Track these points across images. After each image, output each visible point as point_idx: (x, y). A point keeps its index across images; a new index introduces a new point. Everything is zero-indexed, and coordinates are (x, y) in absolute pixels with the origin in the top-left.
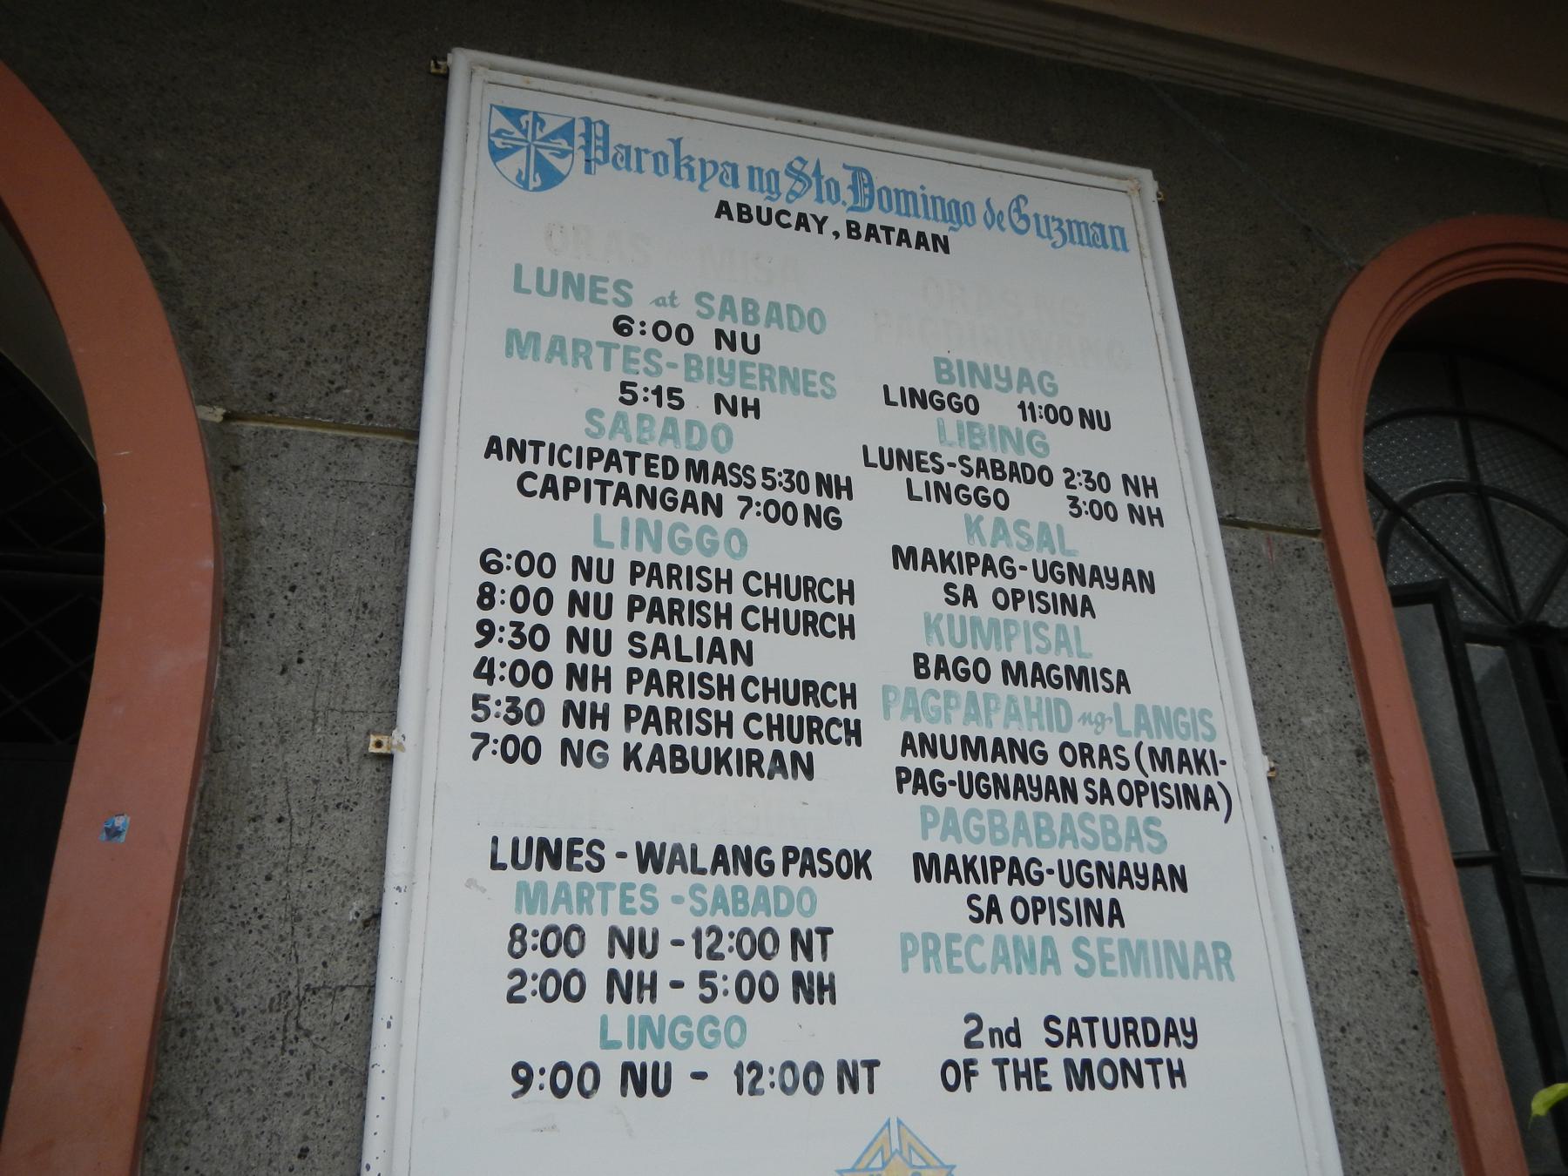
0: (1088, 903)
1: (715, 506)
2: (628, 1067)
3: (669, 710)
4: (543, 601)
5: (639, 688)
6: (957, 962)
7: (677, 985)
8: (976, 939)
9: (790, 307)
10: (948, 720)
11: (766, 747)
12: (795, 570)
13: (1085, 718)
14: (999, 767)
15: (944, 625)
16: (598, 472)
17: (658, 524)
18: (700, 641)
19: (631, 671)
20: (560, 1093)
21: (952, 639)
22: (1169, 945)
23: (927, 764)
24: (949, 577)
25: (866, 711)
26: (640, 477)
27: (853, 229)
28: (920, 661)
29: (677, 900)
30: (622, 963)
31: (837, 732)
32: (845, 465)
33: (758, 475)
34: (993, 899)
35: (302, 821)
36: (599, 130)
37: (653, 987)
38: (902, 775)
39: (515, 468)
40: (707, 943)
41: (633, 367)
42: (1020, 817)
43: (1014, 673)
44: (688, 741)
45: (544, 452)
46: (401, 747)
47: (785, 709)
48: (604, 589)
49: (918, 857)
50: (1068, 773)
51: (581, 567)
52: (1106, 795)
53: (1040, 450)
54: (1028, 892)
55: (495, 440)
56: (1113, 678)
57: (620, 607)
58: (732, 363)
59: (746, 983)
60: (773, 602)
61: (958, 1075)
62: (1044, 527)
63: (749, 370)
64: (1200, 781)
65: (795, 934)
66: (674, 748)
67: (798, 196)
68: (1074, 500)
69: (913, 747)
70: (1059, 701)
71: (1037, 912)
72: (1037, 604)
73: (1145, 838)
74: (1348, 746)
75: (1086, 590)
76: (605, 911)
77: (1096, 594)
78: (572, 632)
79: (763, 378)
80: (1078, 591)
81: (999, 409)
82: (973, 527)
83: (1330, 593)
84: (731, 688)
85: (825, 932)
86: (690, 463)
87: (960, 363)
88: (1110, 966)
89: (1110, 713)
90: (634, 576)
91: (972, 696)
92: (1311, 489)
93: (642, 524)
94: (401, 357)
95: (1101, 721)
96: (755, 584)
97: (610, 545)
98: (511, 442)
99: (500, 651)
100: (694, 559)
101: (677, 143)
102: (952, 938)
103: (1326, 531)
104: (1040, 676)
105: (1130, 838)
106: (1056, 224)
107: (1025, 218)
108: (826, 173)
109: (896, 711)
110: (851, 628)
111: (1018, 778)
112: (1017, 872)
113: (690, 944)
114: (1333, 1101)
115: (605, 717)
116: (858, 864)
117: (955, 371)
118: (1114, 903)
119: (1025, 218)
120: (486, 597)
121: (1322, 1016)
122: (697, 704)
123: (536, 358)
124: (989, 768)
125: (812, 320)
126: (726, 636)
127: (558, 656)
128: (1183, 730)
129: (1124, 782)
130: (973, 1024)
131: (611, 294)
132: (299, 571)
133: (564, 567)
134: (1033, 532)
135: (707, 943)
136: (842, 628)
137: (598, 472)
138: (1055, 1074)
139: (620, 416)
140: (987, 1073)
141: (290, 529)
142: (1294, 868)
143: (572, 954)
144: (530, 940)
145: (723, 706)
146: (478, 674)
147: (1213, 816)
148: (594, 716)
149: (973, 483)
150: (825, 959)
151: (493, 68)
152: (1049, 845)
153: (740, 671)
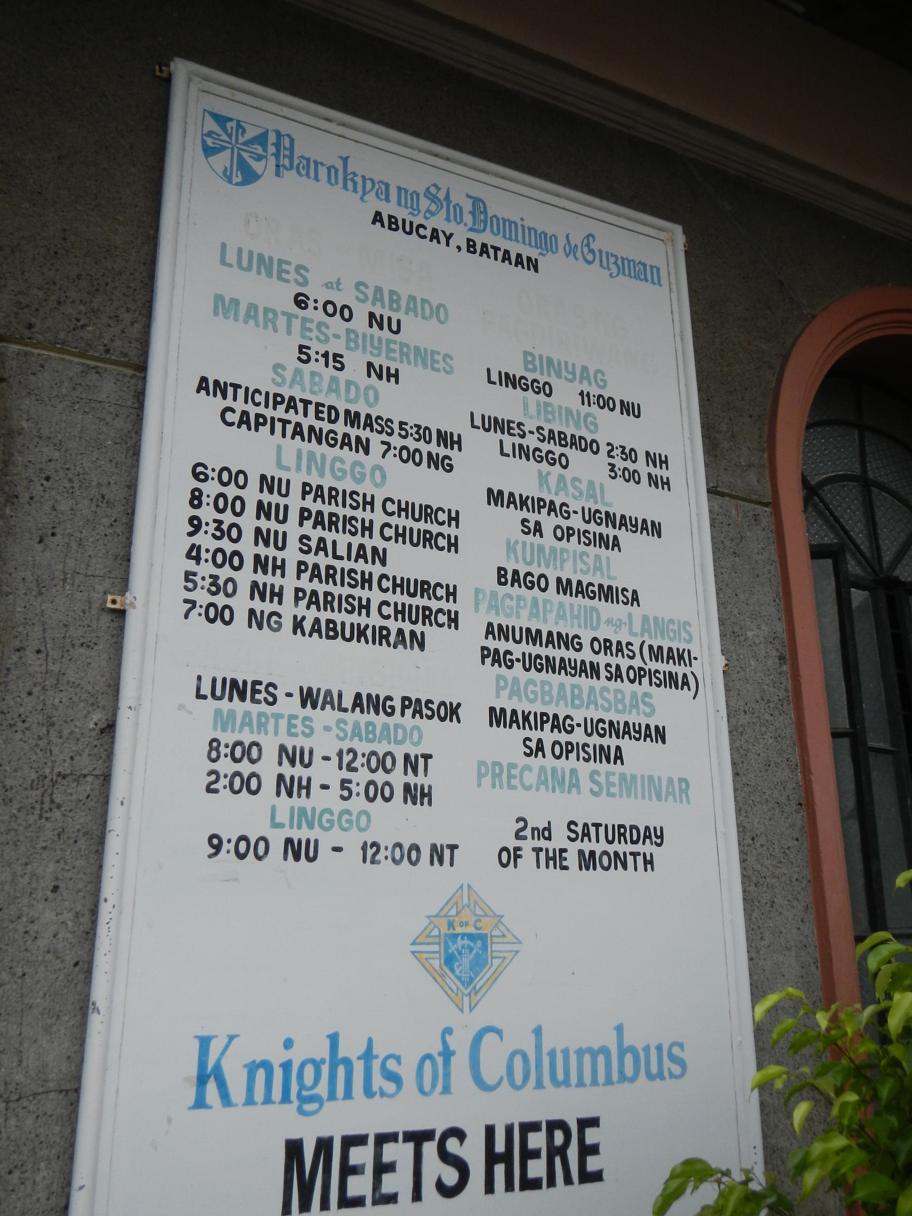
0: (601, 747)
1: (364, 446)
2: (289, 841)
3: (326, 594)
4: (237, 506)
5: (306, 576)
6: (514, 782)
7: (325, 787)
8: (528, 768)
9: (424, 301)
10: (518, 616)
11: (393, 625)
12: (419, 499)
13: (609, 622)
14: (550, 652)
15: (519, 548)
16: (280, 412)
17: (323, 456)
18: (350, 545)
19: (300, 563)
20: (241, 856)
21: (524, 559)
22: (651, 778)
23: (502, 646)
24: (524, 514)
25: (462, 606)
26: (311, 420)
27: (471, 246)
29: (327, 729)
30: (287, 770)
31: (442, 619)
32: (458, 425)
33: (396, 426)
34: (540, 741)
35: (54, 654)
36: (287, 142)
37: (308, 787)
38: (485, 653)
39: (219, 403)
41: (308, 334)
42: (562, 686)
43: (564, 586)
44: (338, 617)
45: (241, 393)
46: (132, 605)
47: (408, 600)
49: (492, 710)
50: (595, 659)
52: (619, 676)
53: (592, 428)
54: (563, 737)
55: (204, 380)
56: (629, 595)
57: (293, 515)
58: (380, 339)
59: (372, 789)
60: (403, 522)
62: (591, 484)
63: (392, 346)
64: (680, 670)
65: (407, 757)
66: (329, 621)
67: (433, 214)
68: (613, 466)
69: (493, 633)
70: (593, 609)
71: (568, 752)
72: (583, 539)
73: (641, 706)
75: (616, 532)
76: (276, 733)
77: (623, 535)
78: (258, 531)
80: (610, 532)
82: (543, 479)
83: (773, 547)
84: (370, 581)
85: (427, 757)
86: (347, 412)
87: (541, 357)
88: (612, 790)
89: (625, 619)
90: (304, 494)
91: (535, 599)
92: (767, 473)
93: (311, 455)
95: (619, 625)
96: (391, 507)
97: (288, 469)
98: (216, 383)
99: (205, 540)
100: (347, 485)
101: (345, 160)
102: (512, 766)
103: (774, 504)
104: (582, 590)
105: (632, 706)
107: (592, 251)
108: (454, 199)
109: (483, 606)
110: (456, 545)
111: (562, 660)
112: (557, 724)
113: (335, 759)
115: (280, 595)
116: (452, 712)
117: (537, 363)
119: (592, 251)
120: (196, 499)
121: (742, 829)
122: (346, 591)
123: (236, 319)
124: (544, 651)
125: (438, 312)
126: (369, 544)
127: (248, 548)
128: (672, 635)
129: (631, 667)
130: (521, 824)
131: (293, 276)
132: (52, 465)
134: (584, 486)
137: (280, 412)
138: (572, 859)
139: (297, 372)
140: (528, 857)
141: (45, 432)
142: (734, 731)
143: (253, 762)
144: (223, 750)
145: (365, 594)
146: (189, 556)
148: (273, 594)
149: (545, 447)
150: (426, 776)
151: (207, 79)
152: (578, 707)
153: (377, 570)
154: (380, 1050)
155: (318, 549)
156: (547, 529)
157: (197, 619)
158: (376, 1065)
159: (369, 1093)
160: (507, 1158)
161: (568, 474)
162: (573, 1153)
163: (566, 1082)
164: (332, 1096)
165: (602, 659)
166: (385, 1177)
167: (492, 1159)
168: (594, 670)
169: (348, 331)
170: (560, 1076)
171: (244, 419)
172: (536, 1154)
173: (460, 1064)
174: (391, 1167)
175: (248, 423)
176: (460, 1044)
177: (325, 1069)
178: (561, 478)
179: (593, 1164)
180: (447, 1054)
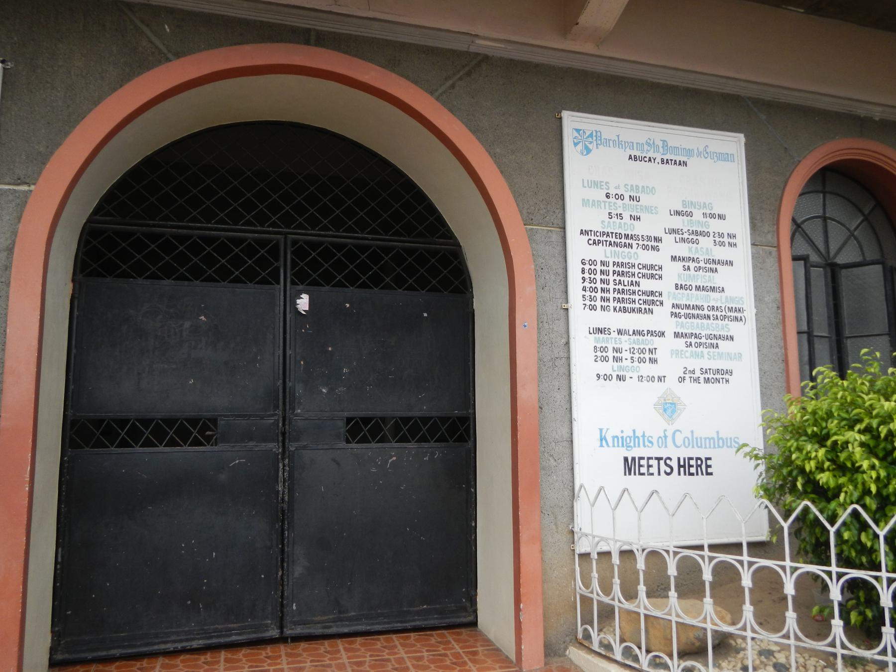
0: (711, 344)
2: (618, 375)
3: (622, 298)
4: (594, 272)
5: (616, 293)
6: (683, 356)
7: (626, 359)
8: (687, 351)
9: (647, 187)
10: (682, 300)
11: (643, 307)
12: (649, 263)
13: (714, 299)
15: (682, 276)
17: (618, 251)
19: (614, 289)
20: (605, 380)
22: (728, 354)
23: (677, 311)
24: (684, 263)
25: (664, 298)
26: (614, 240)
28: (676, 285)
29: (626, 341)
30: (616, 355)
31: (658, 303)
32: (660, 233)
33: (640, 237)
34: (691, 342)
35: (551, 323)
37: (622, 359)
39: (587, 238)
40: (632, 351)
42: (698, 323)
43: (698, 288)
44: (627, 305)
45: (593, 233)
46: (571, 307)
47: (647, 298)
48: (607, 269)
49: (675, 333)
51: (603, 263)
54: (698, 341)
55: (582, 230)
56: (721, 289)
58: (633, 205)
60: (644, 271)
61: (682, 380)
62: (707, 249)
63: (638, 207)
64: (739, 315)
65: (649, 349)
66: (624, 307)
68: (715, 241)
70: (708, 295)
73: (725, 329)
74: (776, 306)
75: (716, 266)
76: (612, 343)
77: (719, 267)
79: (641, 209)
80: (713, 266)
81: (698, 215)
82: (690, 249)
84: (635, 293)
85: (655, 349)
90: (614, 265)
91: (688, 294)
92: (775, 235)
94: (558, 207)
95: (716, 300)
96: (640, 267)
97: (608, 257)
99: (587, 284)
100: (626, 261)
102: (682, 351)
103: (778, 247)
104: (704, 289)
105: (722, 329)
106: (715, 154)
107: (707, 153)
108: (656, 143)
109: (671, 298)
110: (661, 277)
111: (698, 314)
113: (629, 351)
114: (761, 388)
116: (662, 334)
118: (717, 344)
119: (707, 153)
120: (583, 271)
121: (760, 370)
122: (628, 296)
123: (589, 207)
125: (652, 191)
126: (634, 280)
127: (599, 285)
129: (721, 315)
131: (605, 187)
133: (599, 263)
134: (704, 250)
135: (632, 351)
136: (660, 277)
137: (605, 238)
138: (702, 380)
139: (609, 222)
140: (688, 379)
142: (759, 335)
143: (606, 352)
144: (598, 349)
146: (583, 290)
147: (741, 323)
148: (607, 300)
149: (691, 237)
152: (703, 330)
153: (637, 289)
154: (647, 434)
155: (619, 283)
156: (692, 268)
158: (646, 438)
159: (644, 446)
160: (684, 466)
161: (699, 246)
162: (704, 467)
163: (701, 447)
164: (635, 446)
165: (711, 313)
166: (650, 468)
167: (680, 466)
168: (709, 317)
169: (623, 204)
170: (699, 445)
171: (595, 243)
172: (692, 466)
173: (669, 440)
174: (651, 466)
175: (595, 243)
176: (669, 434)
177: (632, 439)
178: (697, 248)
179: (710, 470)
180: (666, 437)
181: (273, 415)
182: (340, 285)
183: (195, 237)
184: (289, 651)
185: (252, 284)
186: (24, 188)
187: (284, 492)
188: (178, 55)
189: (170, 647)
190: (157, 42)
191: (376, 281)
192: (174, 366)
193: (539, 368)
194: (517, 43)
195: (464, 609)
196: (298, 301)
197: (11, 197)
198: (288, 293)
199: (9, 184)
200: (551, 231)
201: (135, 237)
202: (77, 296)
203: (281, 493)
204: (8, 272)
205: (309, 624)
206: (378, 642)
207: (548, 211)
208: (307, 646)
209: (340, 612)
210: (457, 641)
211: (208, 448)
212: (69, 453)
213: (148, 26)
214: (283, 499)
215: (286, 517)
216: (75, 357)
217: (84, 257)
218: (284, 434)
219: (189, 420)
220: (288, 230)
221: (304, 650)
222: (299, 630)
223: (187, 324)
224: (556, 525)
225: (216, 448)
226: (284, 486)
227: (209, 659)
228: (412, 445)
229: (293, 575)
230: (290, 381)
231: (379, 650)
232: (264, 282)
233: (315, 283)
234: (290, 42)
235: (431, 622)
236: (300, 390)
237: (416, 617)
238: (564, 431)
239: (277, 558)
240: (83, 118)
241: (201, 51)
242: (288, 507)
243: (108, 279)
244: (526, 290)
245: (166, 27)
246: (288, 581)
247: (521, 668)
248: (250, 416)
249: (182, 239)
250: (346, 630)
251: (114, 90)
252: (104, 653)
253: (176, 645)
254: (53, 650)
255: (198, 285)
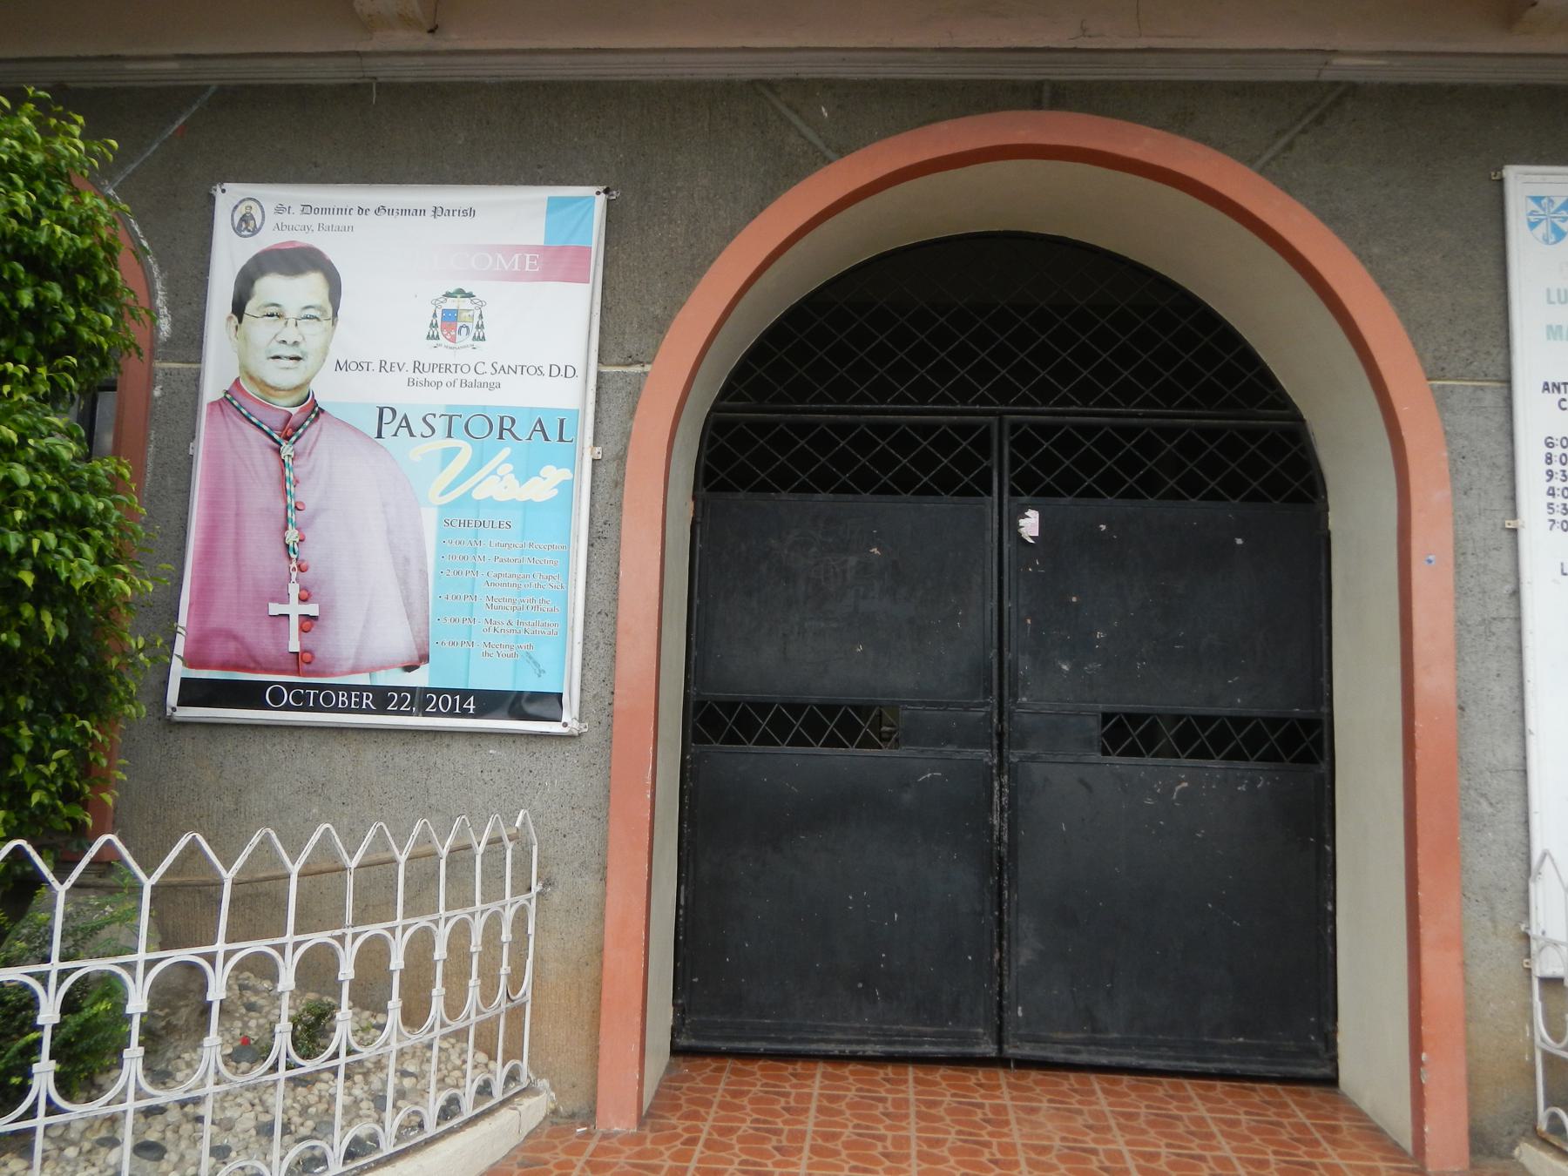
35: (1482, 555)
39: (1556, 397)
46: (1523, 527)
55: (1546, 384)
98: (1554, 385)
120: (1549, 459)
151: (1527, 174)
157: (1557, 530)
181: (983, 705)
182: (1090, 493)
183: (862, 426)
184: (1013, 1080)
185: (949, 497)
186: (637, 369)
187: (1001, 827)
188: (842, 152)
189: (834, 1049)
190: (811, 136)
191: (1150, 485)
192: (834, 625)
193: (1459, 639)
194: (1413, 54)
195: (1313, 1053)
196: (1022, 522)
197: (620, 384)
198: (1006, 508)
199: (618, 365)
200: (1482, 388)
201: (777, 429)
202: (699, 519)
203: (997, 828)
204: (618, 491)
205: (1045, 1042)
206: (1160, 1088)
207: (1476, 352)
208: (1040, 1077)
209: (1094, 1030)
210: (1302, 1105)
211: (885, 752)
212: (693, 750)
213: (797, 112)
214: (1000, 838)
215: (1005, 867)
216: (698, 610)
217: (708, 463)
218: (1000, 735)
219: (856, 708)
220: (1004, 408)
221: (1036, 1082)
222: (1027, 1050)
223: (853, 561)
224: (1493, 920)
225: (896, 753)
226: (1002, 819)
227: (891, 1075)
228: (1216, 764)
229: (1017, 961)
230: (1009, 650)
231: (1161, 1100)
232: (967, 492)
233: (1048, 492)
234: (1009, 107)
235: (1253, 1068)
236: (1025, 666)
237: (1225, 1056)
238: (1509, 752)
239: (992, 931)
240: (712, 262)
241: (874, 141)
242: (1009, 852)
243: (742, 495)
244: (1431, 495)
245: (823, 109)
246: (1009, 967)
247: (1423, 1166)
248: (948, 704)
249: (842, 429)
250: (1104, 1060)
251: (753, 216)
252: (742, 1045)
253: (842, 1047)
254: (675, 1031)
255: (868, 502)
